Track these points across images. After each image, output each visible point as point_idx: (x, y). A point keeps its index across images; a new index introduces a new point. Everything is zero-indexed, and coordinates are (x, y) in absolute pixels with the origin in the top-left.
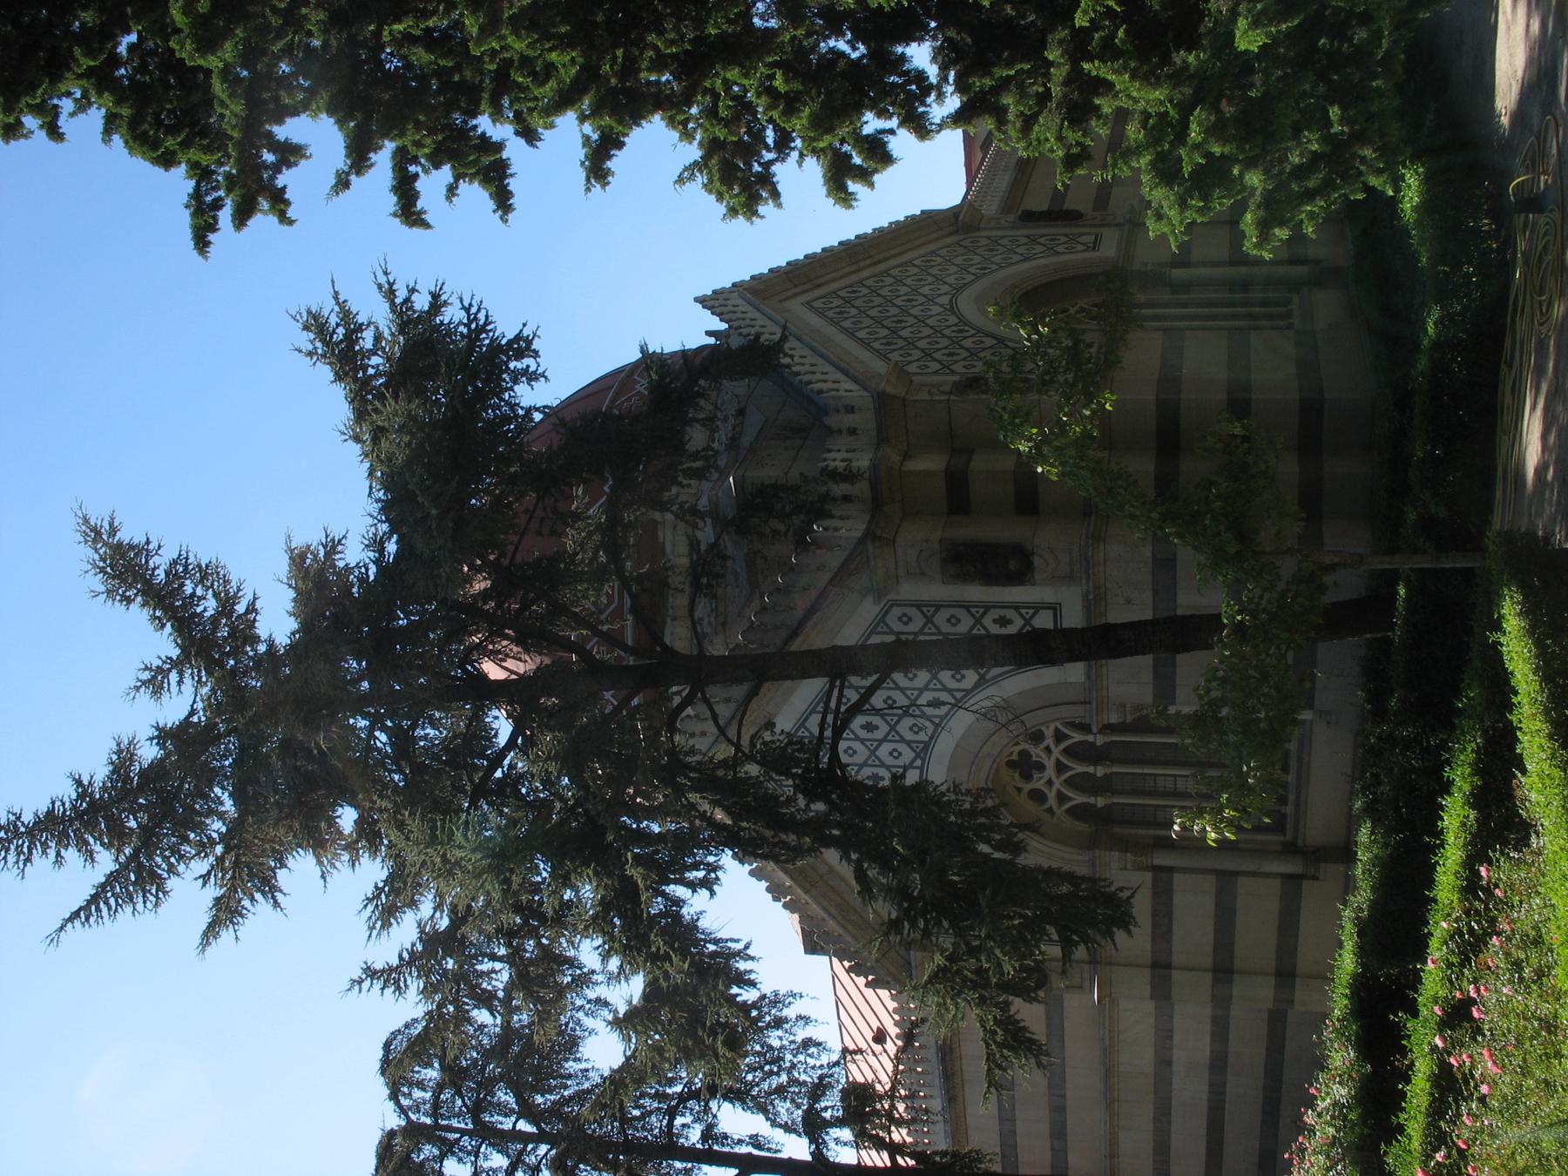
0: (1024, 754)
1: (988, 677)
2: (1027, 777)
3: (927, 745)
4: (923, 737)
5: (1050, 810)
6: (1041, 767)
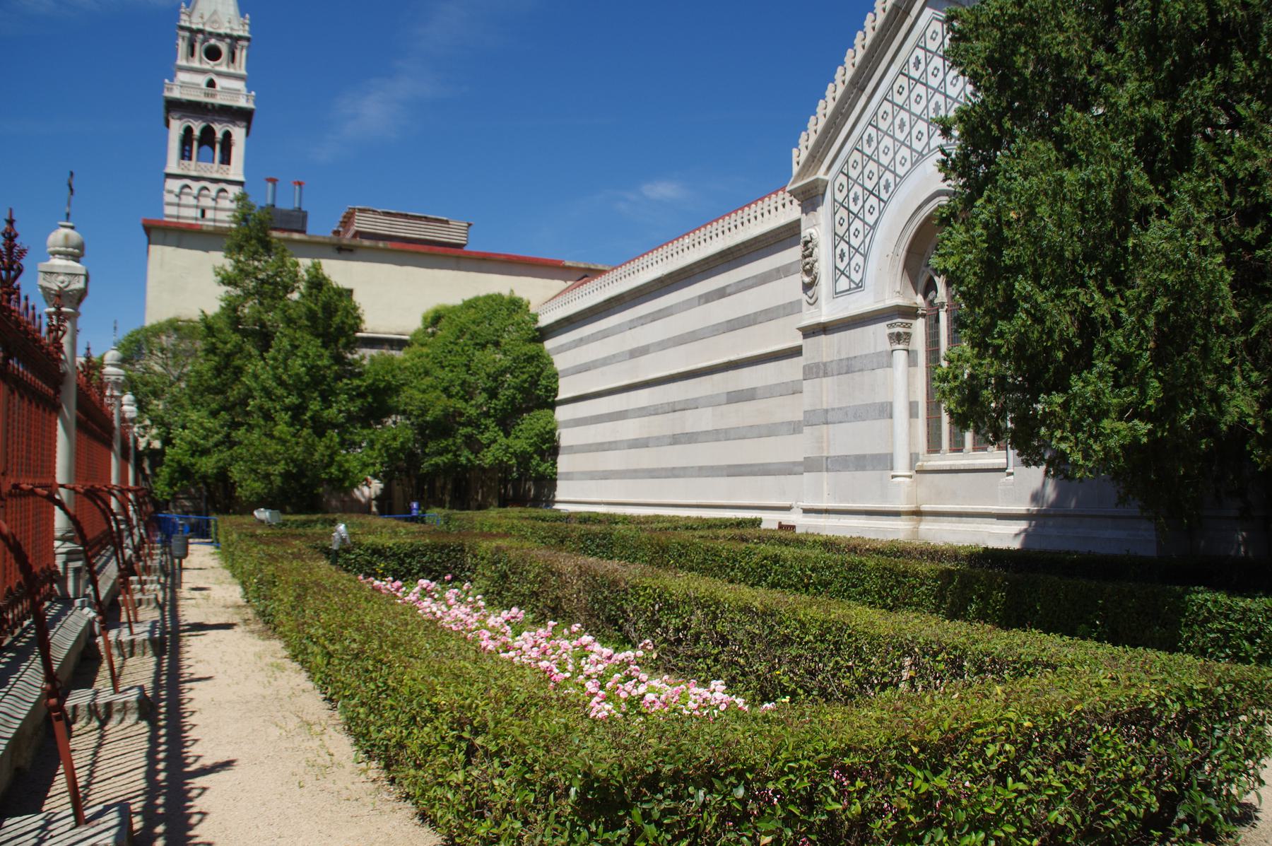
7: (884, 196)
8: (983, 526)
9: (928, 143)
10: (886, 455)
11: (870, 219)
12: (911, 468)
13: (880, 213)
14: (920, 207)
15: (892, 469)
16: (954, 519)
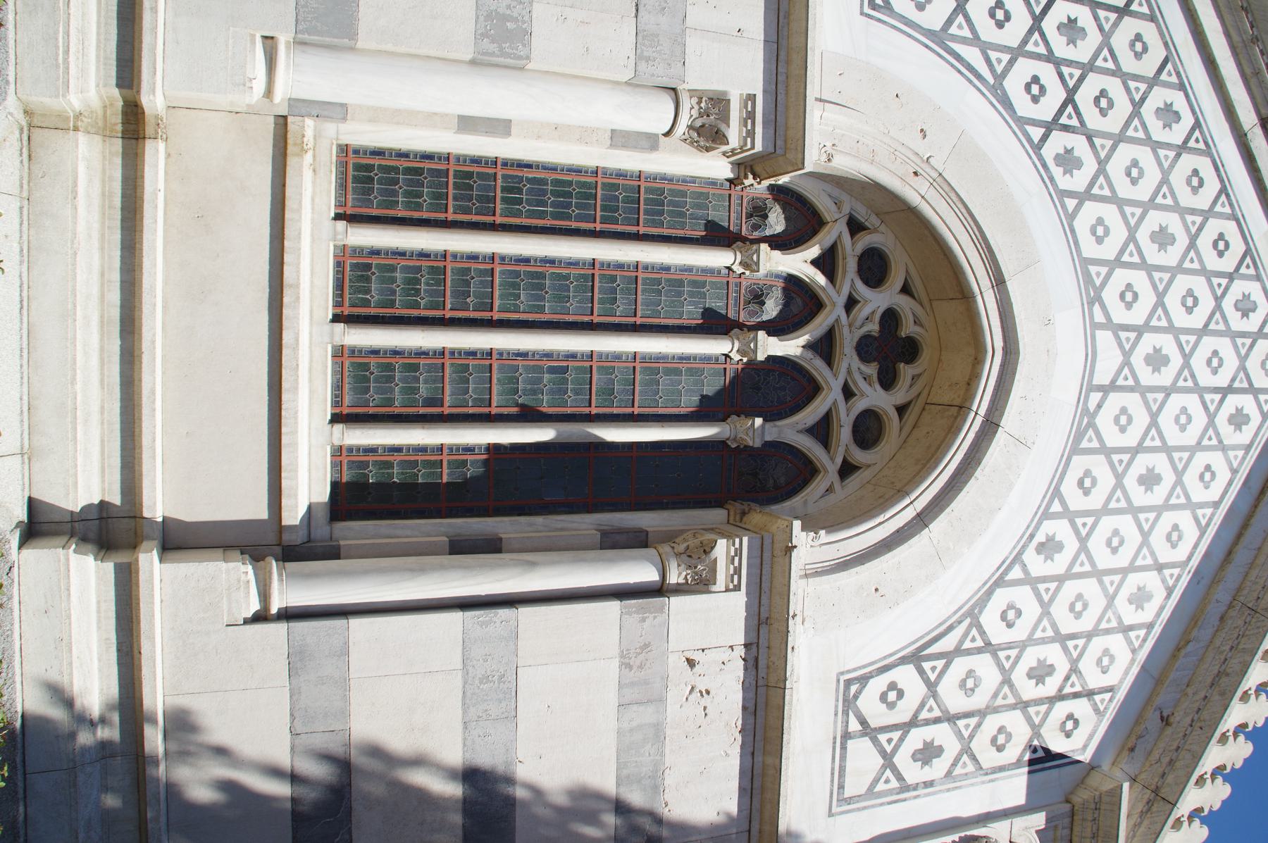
0: (887, 381)
1: (968, 620)
2: (890, 318)
3: (1076, 450)
4: (1079, 464)
5: (855, 227)
6: (865, 348)
7: (1058, 142)
8: (96, 433)
9: (1109, 325)
10: (353, 36)
11: (1014, 85)
12: (293, 102)
13: (1022, 122)
14: (999, 282)
15: (299, 43)
16: (115, 296)
